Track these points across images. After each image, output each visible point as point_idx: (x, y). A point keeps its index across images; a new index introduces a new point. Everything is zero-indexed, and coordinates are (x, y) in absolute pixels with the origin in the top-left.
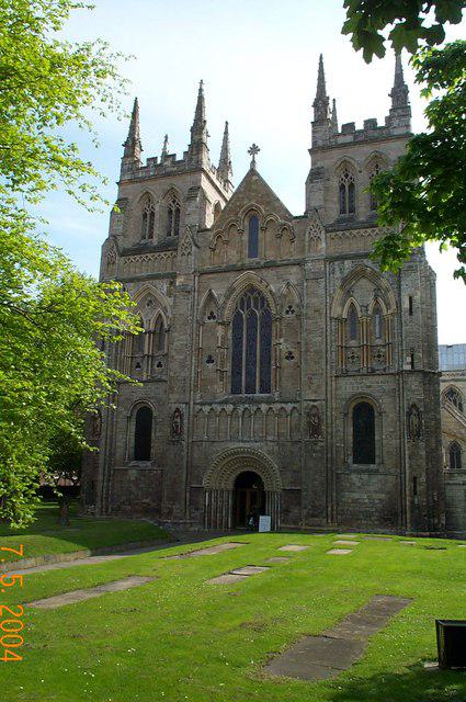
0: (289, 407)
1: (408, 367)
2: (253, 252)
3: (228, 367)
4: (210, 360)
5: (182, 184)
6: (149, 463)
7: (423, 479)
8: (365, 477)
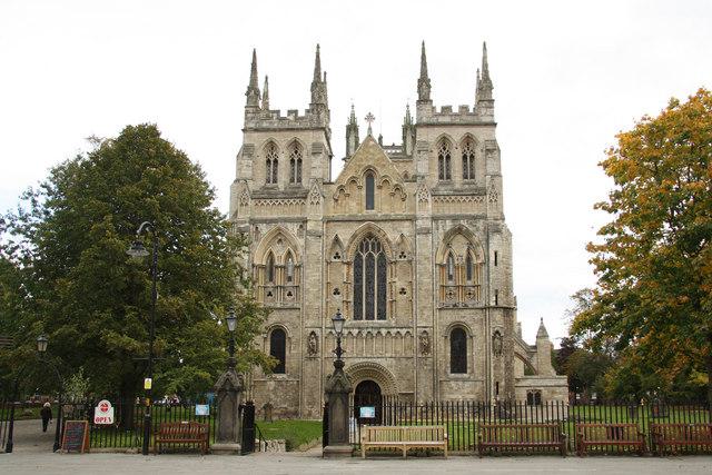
0: (403, 332)
1: (493, 304)
2: (370, 204)
3: (351, 299)
4: (337, 292)
5: (307, 139)
6: (285, 376)
7: (503, 383)
8: (460, 383)
